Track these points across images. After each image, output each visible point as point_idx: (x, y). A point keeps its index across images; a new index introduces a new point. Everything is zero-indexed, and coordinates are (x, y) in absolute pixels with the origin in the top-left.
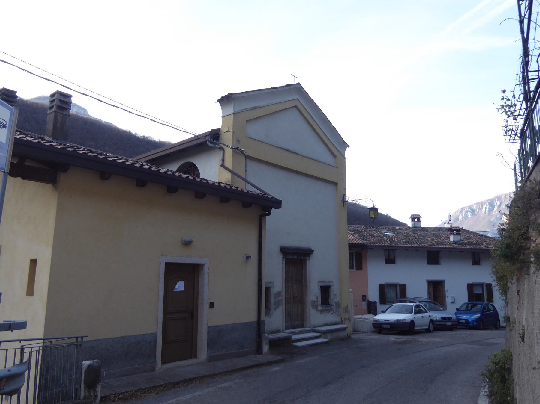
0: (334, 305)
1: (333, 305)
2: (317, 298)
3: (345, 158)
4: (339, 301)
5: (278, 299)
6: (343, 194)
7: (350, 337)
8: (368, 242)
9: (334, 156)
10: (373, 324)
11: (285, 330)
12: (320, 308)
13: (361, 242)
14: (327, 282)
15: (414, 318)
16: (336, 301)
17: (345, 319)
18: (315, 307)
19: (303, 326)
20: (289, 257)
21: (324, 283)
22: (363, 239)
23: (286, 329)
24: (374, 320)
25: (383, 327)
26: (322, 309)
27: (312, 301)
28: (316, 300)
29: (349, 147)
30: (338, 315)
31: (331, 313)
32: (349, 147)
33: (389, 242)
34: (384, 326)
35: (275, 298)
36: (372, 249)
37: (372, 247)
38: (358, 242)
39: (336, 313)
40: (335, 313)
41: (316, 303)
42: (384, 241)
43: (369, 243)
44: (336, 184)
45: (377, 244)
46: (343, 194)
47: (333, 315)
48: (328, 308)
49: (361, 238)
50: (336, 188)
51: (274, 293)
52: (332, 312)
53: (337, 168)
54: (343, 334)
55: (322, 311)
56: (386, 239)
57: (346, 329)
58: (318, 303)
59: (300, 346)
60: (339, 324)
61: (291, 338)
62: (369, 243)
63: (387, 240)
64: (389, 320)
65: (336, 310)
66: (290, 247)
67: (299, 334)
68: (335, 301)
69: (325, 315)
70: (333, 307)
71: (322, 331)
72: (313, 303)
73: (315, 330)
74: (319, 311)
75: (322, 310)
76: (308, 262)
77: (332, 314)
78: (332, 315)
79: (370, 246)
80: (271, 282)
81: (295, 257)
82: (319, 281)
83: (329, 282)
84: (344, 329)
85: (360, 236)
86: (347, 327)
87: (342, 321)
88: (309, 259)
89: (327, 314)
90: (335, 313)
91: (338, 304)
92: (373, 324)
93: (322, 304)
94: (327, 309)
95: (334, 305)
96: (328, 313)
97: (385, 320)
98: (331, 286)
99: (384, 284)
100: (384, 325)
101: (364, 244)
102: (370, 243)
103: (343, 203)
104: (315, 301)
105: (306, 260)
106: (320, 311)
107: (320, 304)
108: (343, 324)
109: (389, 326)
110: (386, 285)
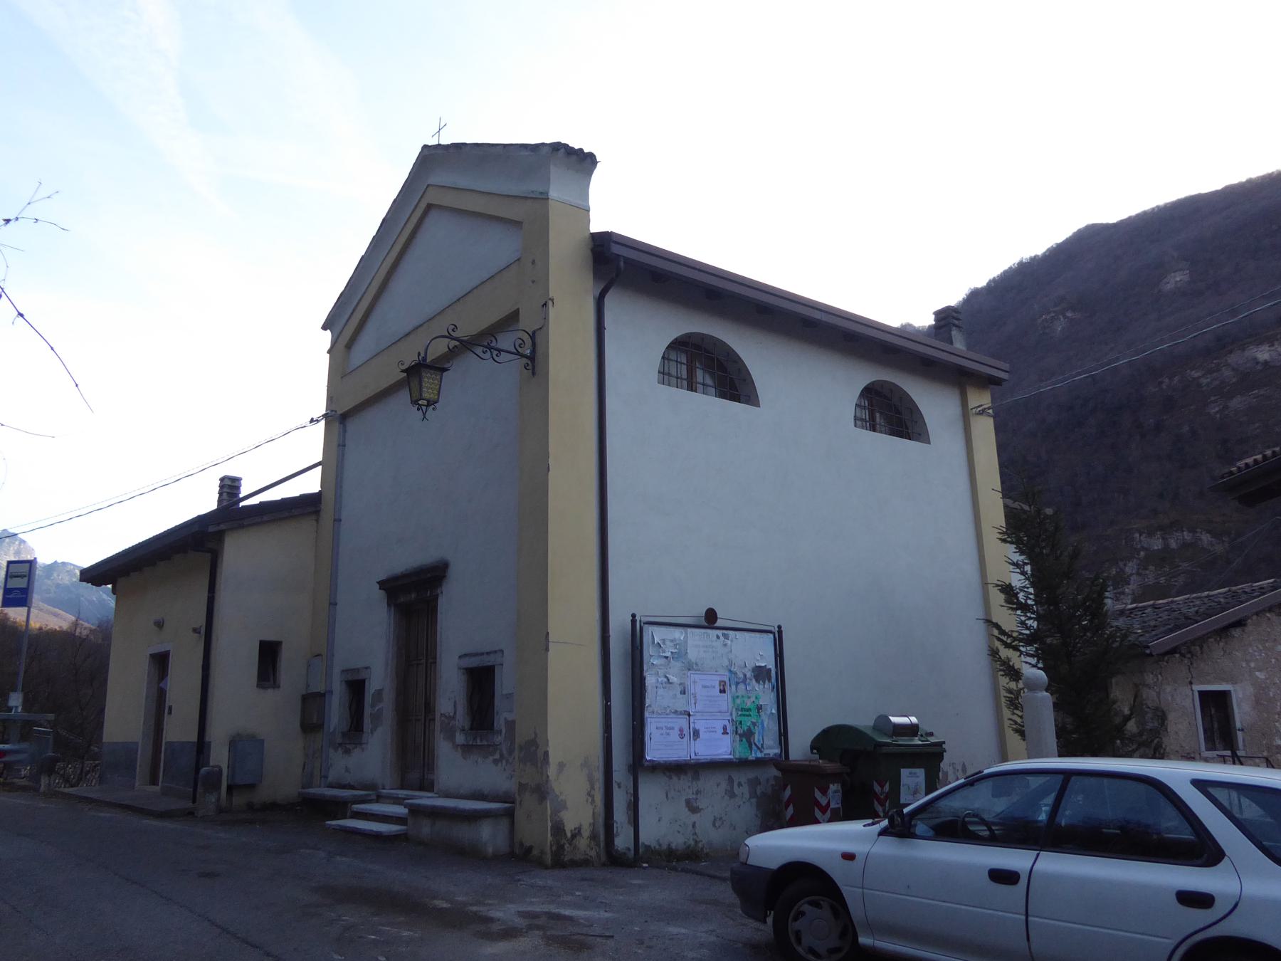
0: (504, 731)
5: (377, 708)
12: (460, 738)
14: (482, 654)
15: (849, 857)
18: (450, 737)
20: (402, 600)
26: (465, 743)
28: (452, 714)
35: (373, 706)
39: (507, 761)
40: (504, 762)
47: (500, 764)
52: (497, 756)
55: (467, 749)
68: (505, 719)
70: (498, 739)
72: (446, 721)
74: (459, 749)
75: (464, 745)
77: (496, 762)
78: (497, 765)
80: (366, 668)
81: (413, 596)
89: (480, 760)
90: (504, 762)
95: (504, 731)
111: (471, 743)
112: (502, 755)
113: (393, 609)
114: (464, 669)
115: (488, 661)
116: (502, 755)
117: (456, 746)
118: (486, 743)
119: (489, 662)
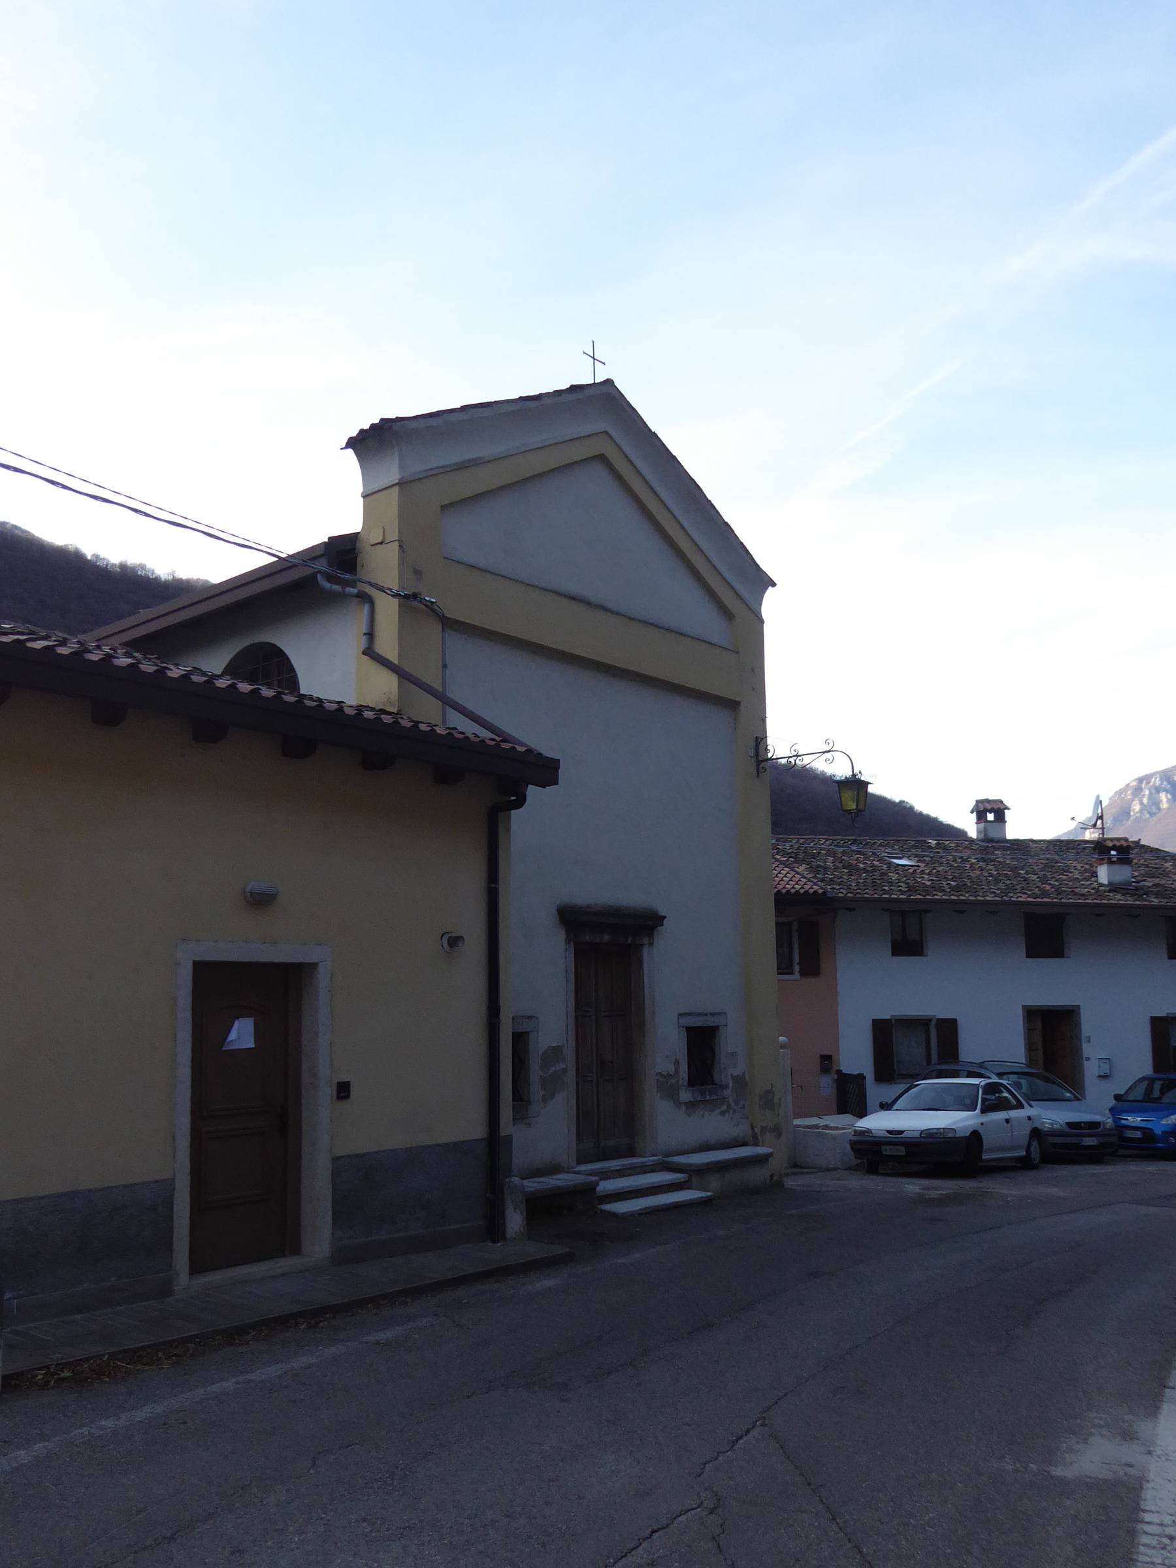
0: (731, 1085)
1: (727, 1086)
2: (677, 1063)
3: (762, 622)
4: (744, 1073)
5: (552, 1070)
6: (757, 738)
7: (780, 1185)
8: (838, 887)
9: (728, 615)
10: (853, 1144)
11: (574, 1163)
12: (685, 1095)
13: (816, 887)
14: (706, 1014)
15: (982, 1124)
16: (737, 1072)
17: (764, 1129)
19: (632, 1153)
21: (700, 1018)
22: (823, 880)
23: (579, 1162)
24: (855, 1131)
25: (884, 1153)
26: (692, 1100)
27: (660, 1074)
28: (672, 1071)
29: (774, 584)
30: (741, 1118)
31: (718, 1111)
32: (774, 584)
33: (904, 887)
34: (887, 1151)
36: (851, 910)
37: (852, 906)
38: (807, 887)
39: (735, 1111)
40: (731, 1112)
41: (673, 1081)
42: (890, 883)
43: (841, 890)
44: (732, 705)
45: (866, 893)
46: (757, 738)
47: (727, 1115)
48: (710, 1095)
49: (815, 877)
50: (735, 719)
51: (541, 1053)
52: (724, 1108)
53: (737, 652)
54: (757, 1175)
55: (691, 1106)
56: (894, 877)
57: (767, 1160)
58: (678, 1081)
59: (623, 1214)
60: (745, 1144)
61: (595, 1189)
62: (841, 890)
63: (899, 880)
64: (901, 1132)
65: (737, 1103)
66: (588, 906)
67: (621, 1176)
68: (732, 1075)
69: (703, 1116)
70: (727, 1092)
71: (690, 1165)
72: (662, 1080)
73: (672, 1163)
76: (645, 951)
77: (723, 1113)
79: (845, 899)
80: (530, 1017)
82: (681, 1012)
83: (713, 1014)
84: (762, 1160)
85: (815, 870)
86: (771, 1155)
87: (755, 1136)
88: (651, 944)
89: (706, 1114)
90: (731, 1112)
91: (741, 1083)
92: (853, 1144)
93: (691, 1084)
94: (708, 1098)
95: (731, 1085)
96: (712, 1110)
97: (890, 1132)
98: (721, 1028)
99: (890, 1020)
100: (888, 1147)
101: (824, 893)
102: (844, 891)
103: (758, 766)
104: (669, 1075)
105: (640, 946)
106: (685, 1103)
107: (686, 1083)
108: (756, 1144)
109: (902, 1151)
110: (893, 1021)
111: (699, 1099)
112: (729, 1106)
113: (572, 945)
114: (686, 1027)
115: (711, 1022)
116: (729, 1106)
117: (678, 1104)
118: (715, 1098)
119: (714, 1022)
